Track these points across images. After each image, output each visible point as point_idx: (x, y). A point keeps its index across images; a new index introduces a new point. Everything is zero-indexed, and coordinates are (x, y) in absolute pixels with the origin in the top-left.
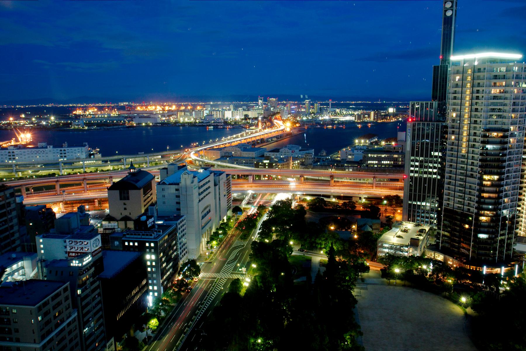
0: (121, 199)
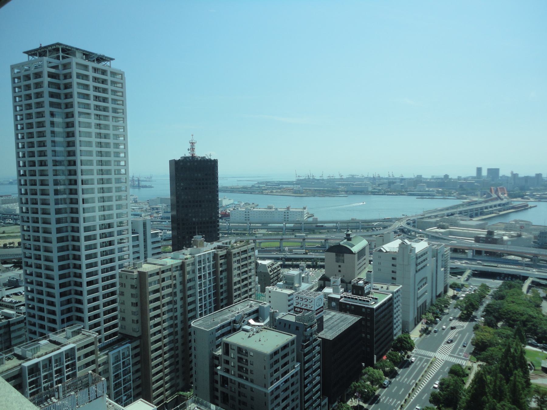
0: (337, 261)
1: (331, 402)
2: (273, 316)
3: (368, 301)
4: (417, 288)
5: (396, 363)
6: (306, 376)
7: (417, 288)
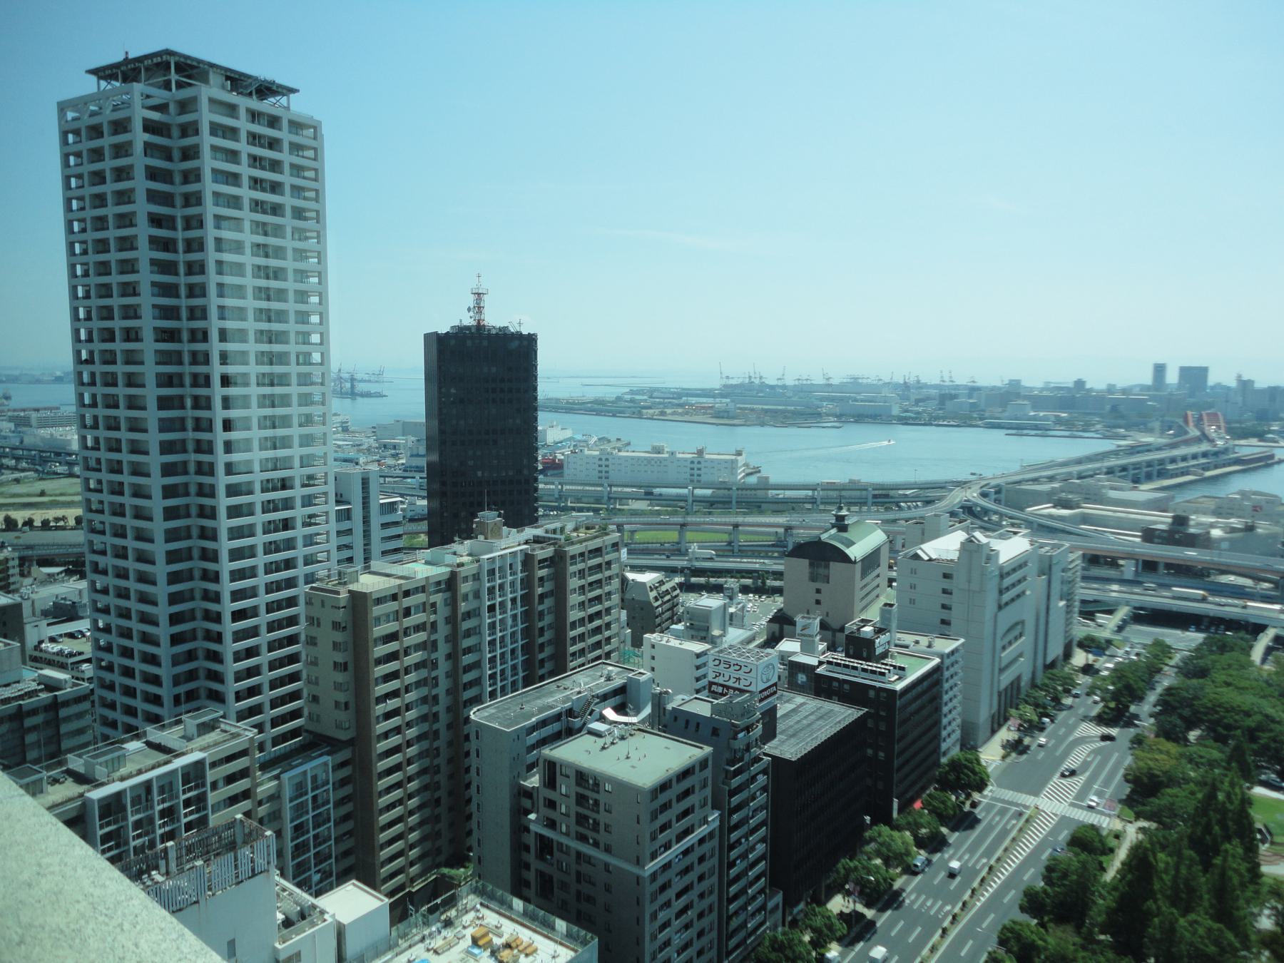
0: (813, 578)
1: (789, 903)
2: (659, 701)
3: (883, 674)
4: (999, 644)
5: (943, 819)
6: (732, 840)
7: (999, 644)
